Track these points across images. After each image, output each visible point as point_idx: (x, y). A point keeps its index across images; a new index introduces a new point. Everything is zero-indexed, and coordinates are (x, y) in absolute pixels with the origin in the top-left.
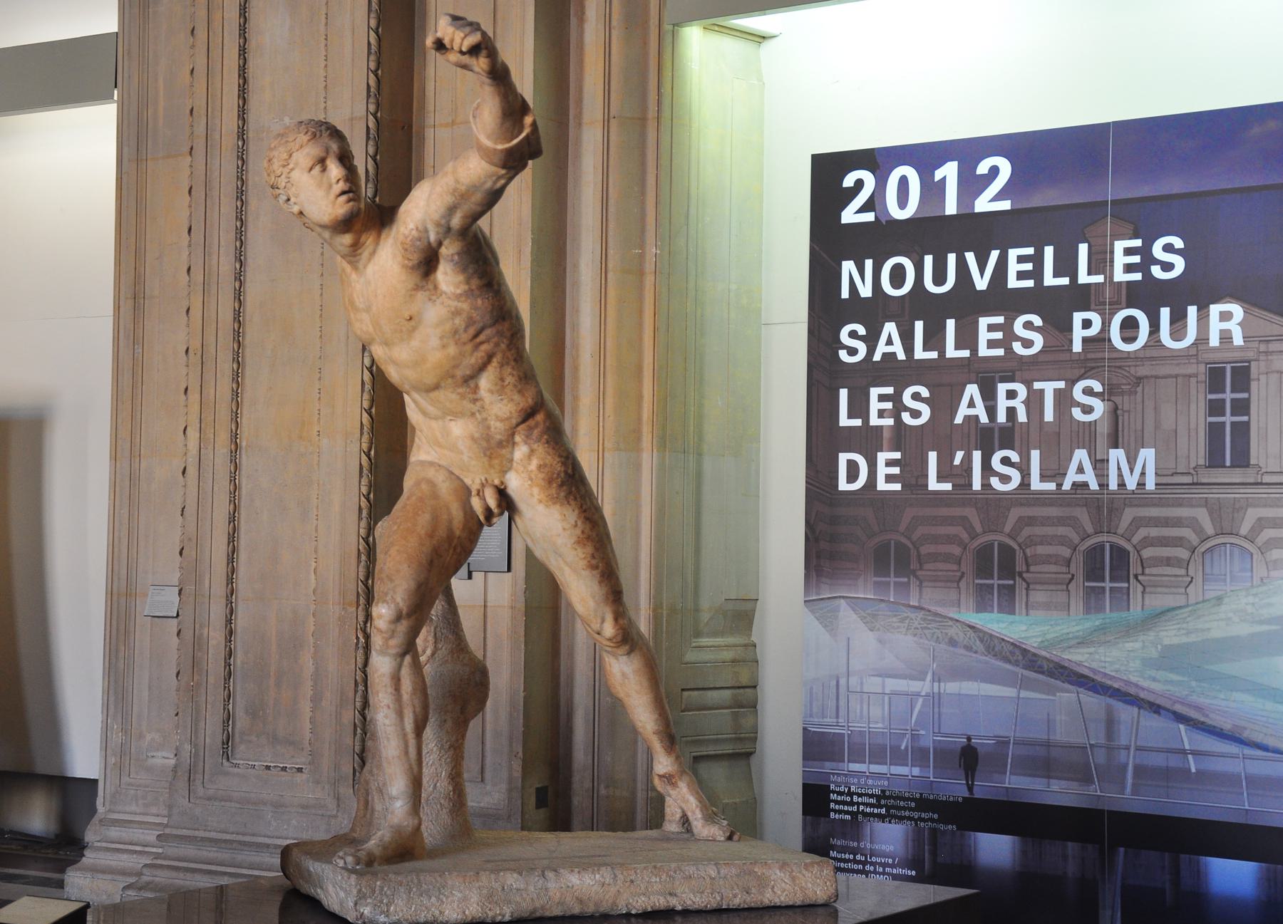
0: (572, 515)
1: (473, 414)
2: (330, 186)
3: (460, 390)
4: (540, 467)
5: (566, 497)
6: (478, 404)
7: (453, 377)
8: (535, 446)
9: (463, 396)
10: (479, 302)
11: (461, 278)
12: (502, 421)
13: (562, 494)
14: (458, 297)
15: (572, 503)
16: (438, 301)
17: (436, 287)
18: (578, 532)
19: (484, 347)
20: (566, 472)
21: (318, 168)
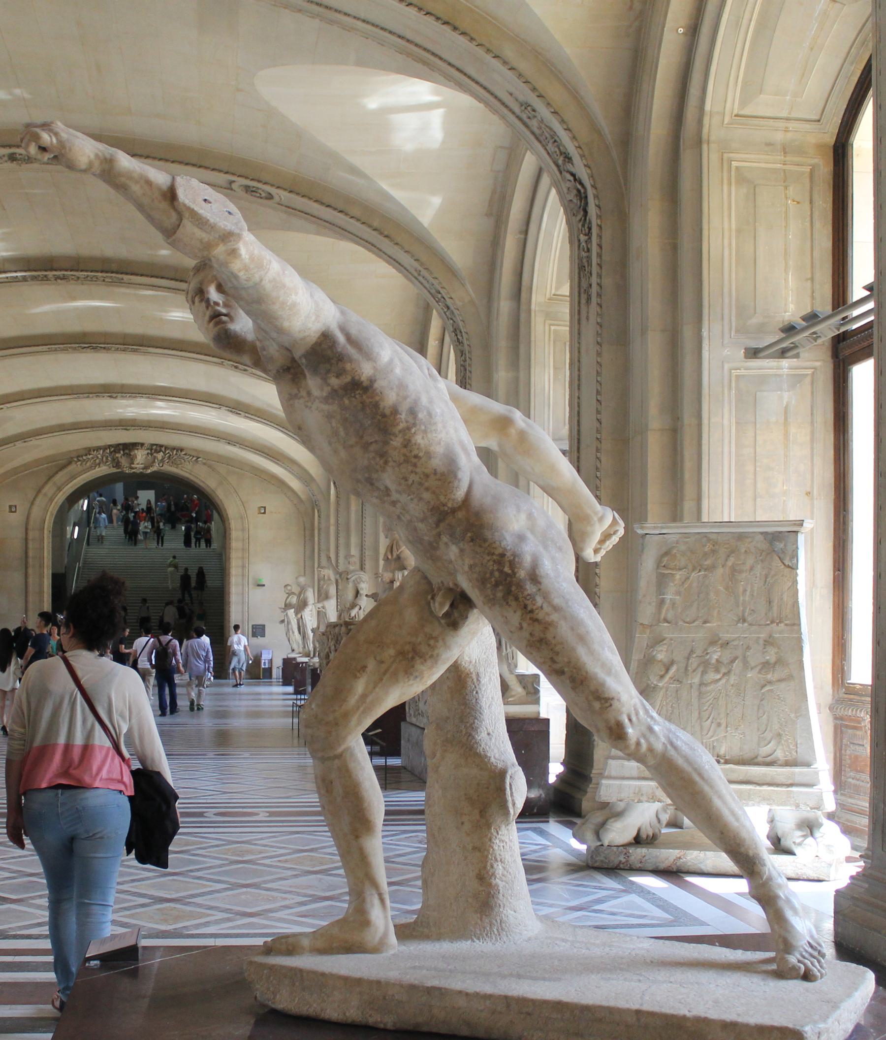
0: (515, 618)
1: (399, 517)
2: (205, 314)
3: (376, 494)
4: (471, 567)
5: (505, 598)
6: (399, 505)
7: (358, 481)
8: (461, 545)
9: (383, 502)
10: (347, 402)
11: (318, 381)
12: (422, 521)
13: (499, 595)
14: (326, 400)
15: (513, 603)
16: (314, 407)
17: (309, 394)
18: (525, 634)
19: (373, 447)
20: (501, 571)
21: (197, 299)
